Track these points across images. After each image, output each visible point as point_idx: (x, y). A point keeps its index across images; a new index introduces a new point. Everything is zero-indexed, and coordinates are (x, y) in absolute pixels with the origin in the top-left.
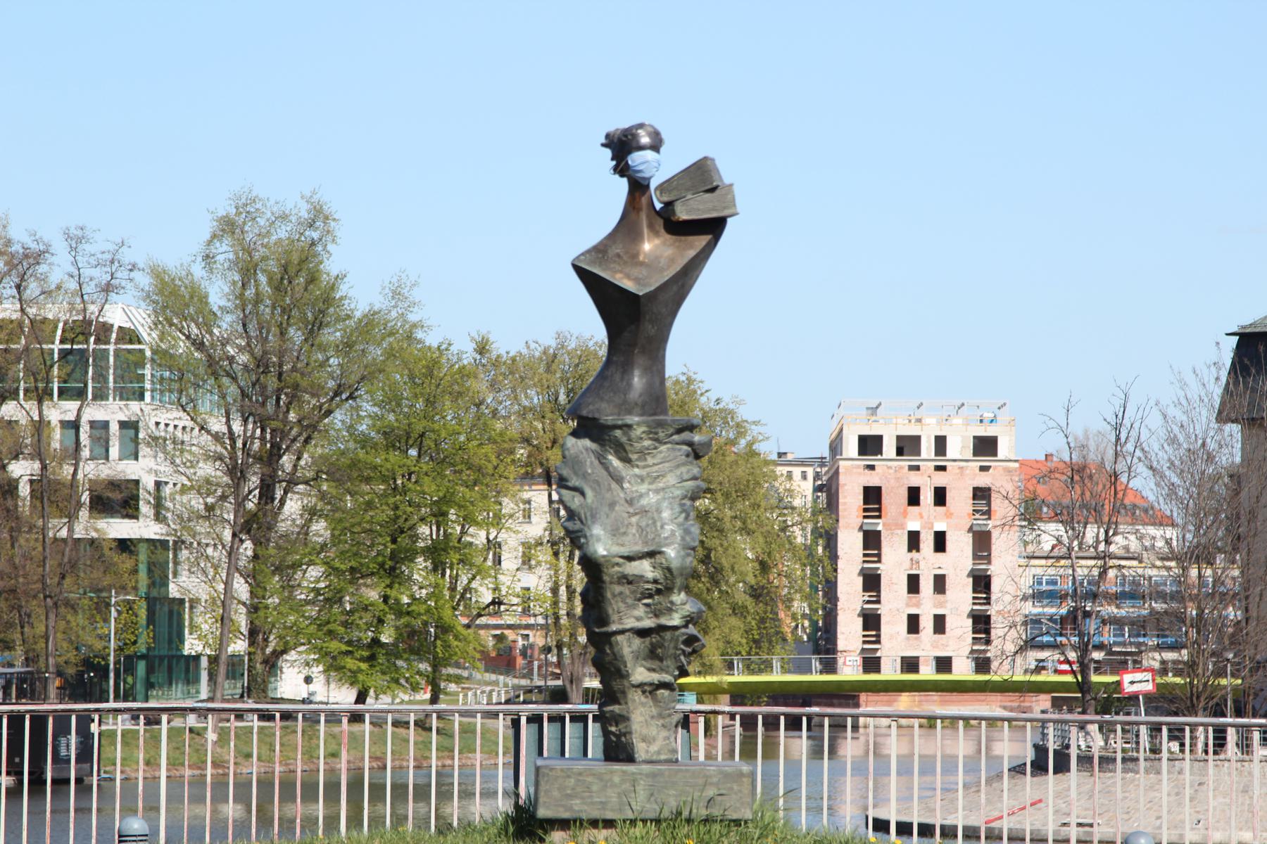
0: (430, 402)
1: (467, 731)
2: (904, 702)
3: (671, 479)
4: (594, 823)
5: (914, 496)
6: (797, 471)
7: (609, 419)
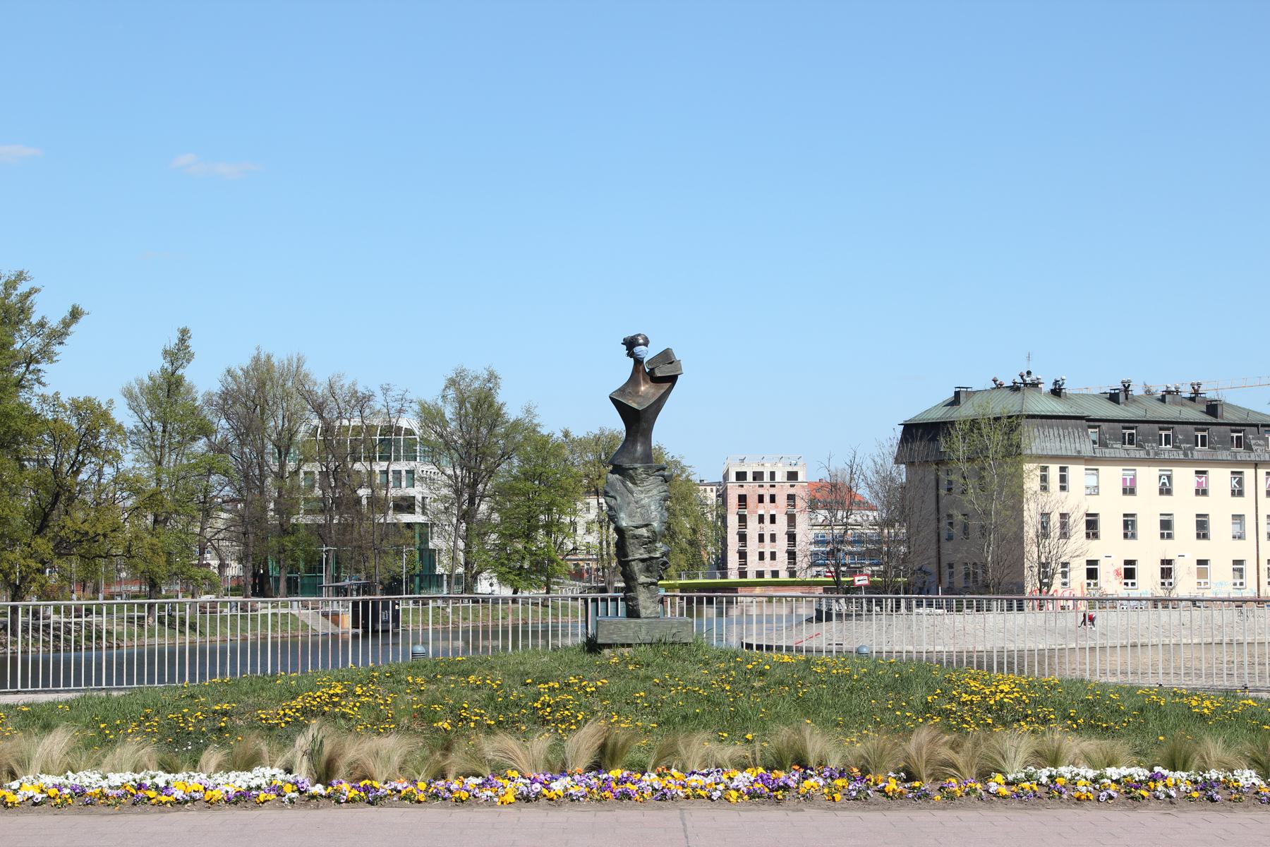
0: (544, 459)
1: (565, 607)
2: (758, 590)
3: (655, 492)
4: (623, 645)
5: (761, 499)
6: (708, 488)
7: (627, 466)
